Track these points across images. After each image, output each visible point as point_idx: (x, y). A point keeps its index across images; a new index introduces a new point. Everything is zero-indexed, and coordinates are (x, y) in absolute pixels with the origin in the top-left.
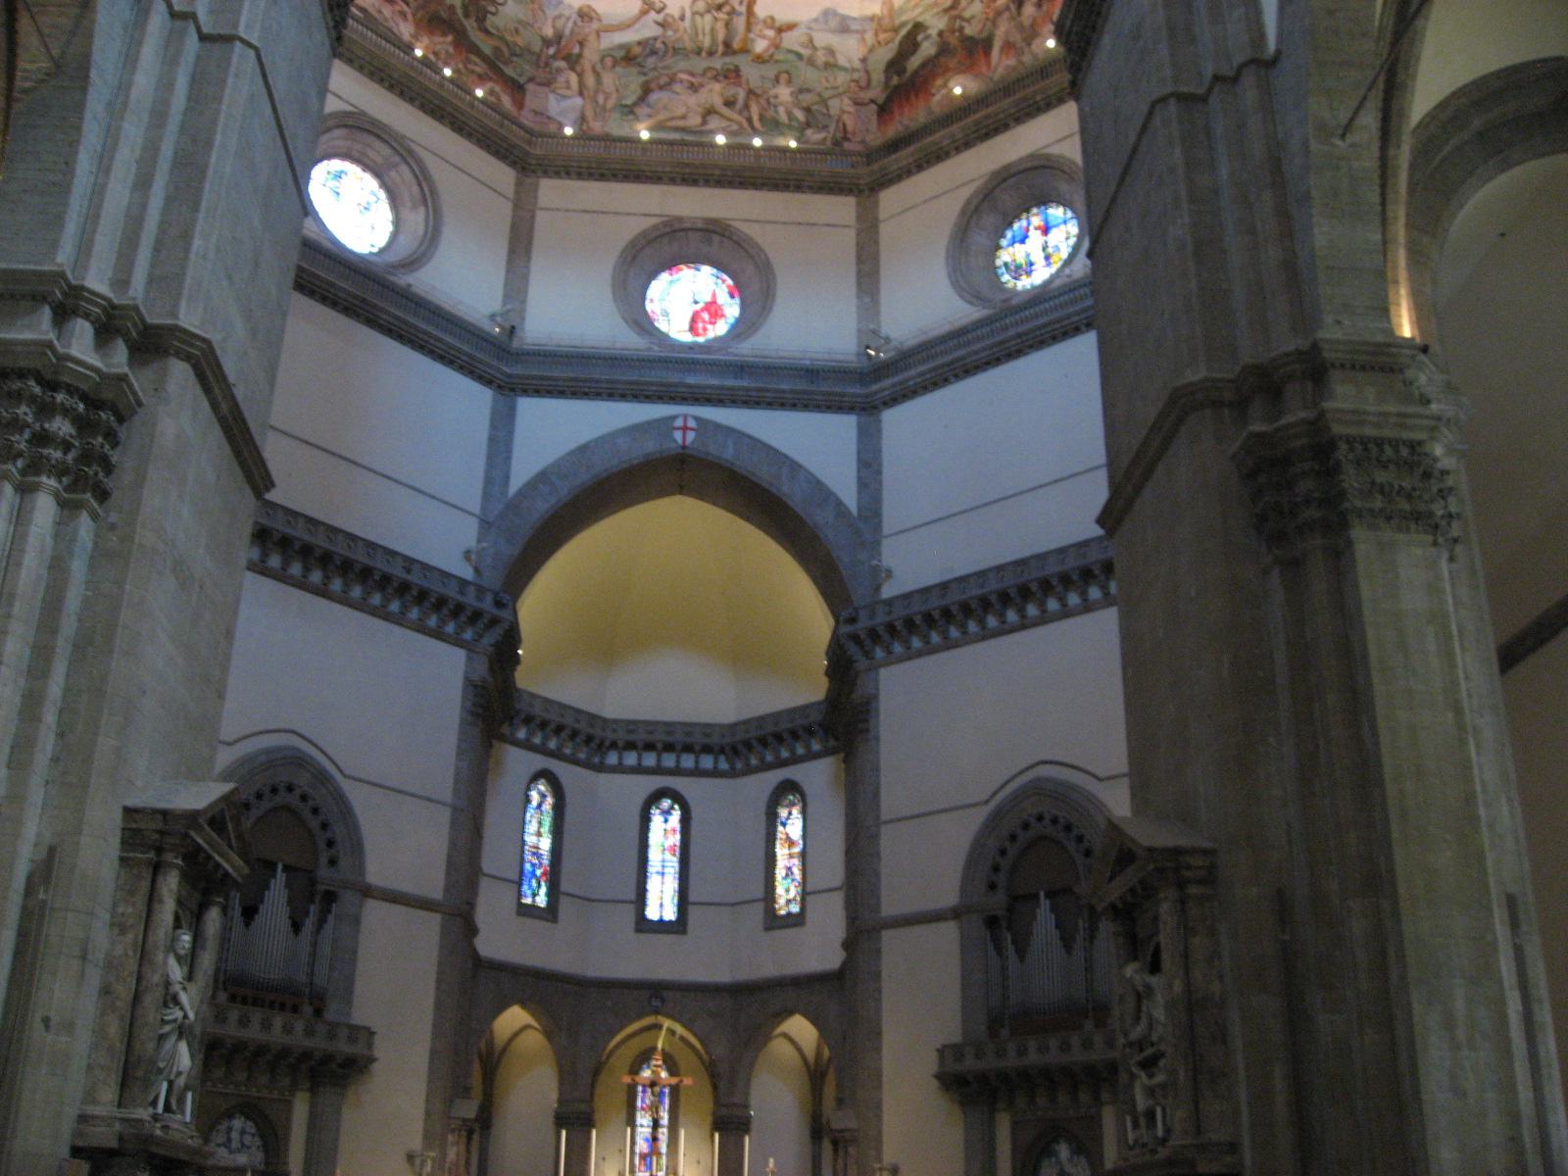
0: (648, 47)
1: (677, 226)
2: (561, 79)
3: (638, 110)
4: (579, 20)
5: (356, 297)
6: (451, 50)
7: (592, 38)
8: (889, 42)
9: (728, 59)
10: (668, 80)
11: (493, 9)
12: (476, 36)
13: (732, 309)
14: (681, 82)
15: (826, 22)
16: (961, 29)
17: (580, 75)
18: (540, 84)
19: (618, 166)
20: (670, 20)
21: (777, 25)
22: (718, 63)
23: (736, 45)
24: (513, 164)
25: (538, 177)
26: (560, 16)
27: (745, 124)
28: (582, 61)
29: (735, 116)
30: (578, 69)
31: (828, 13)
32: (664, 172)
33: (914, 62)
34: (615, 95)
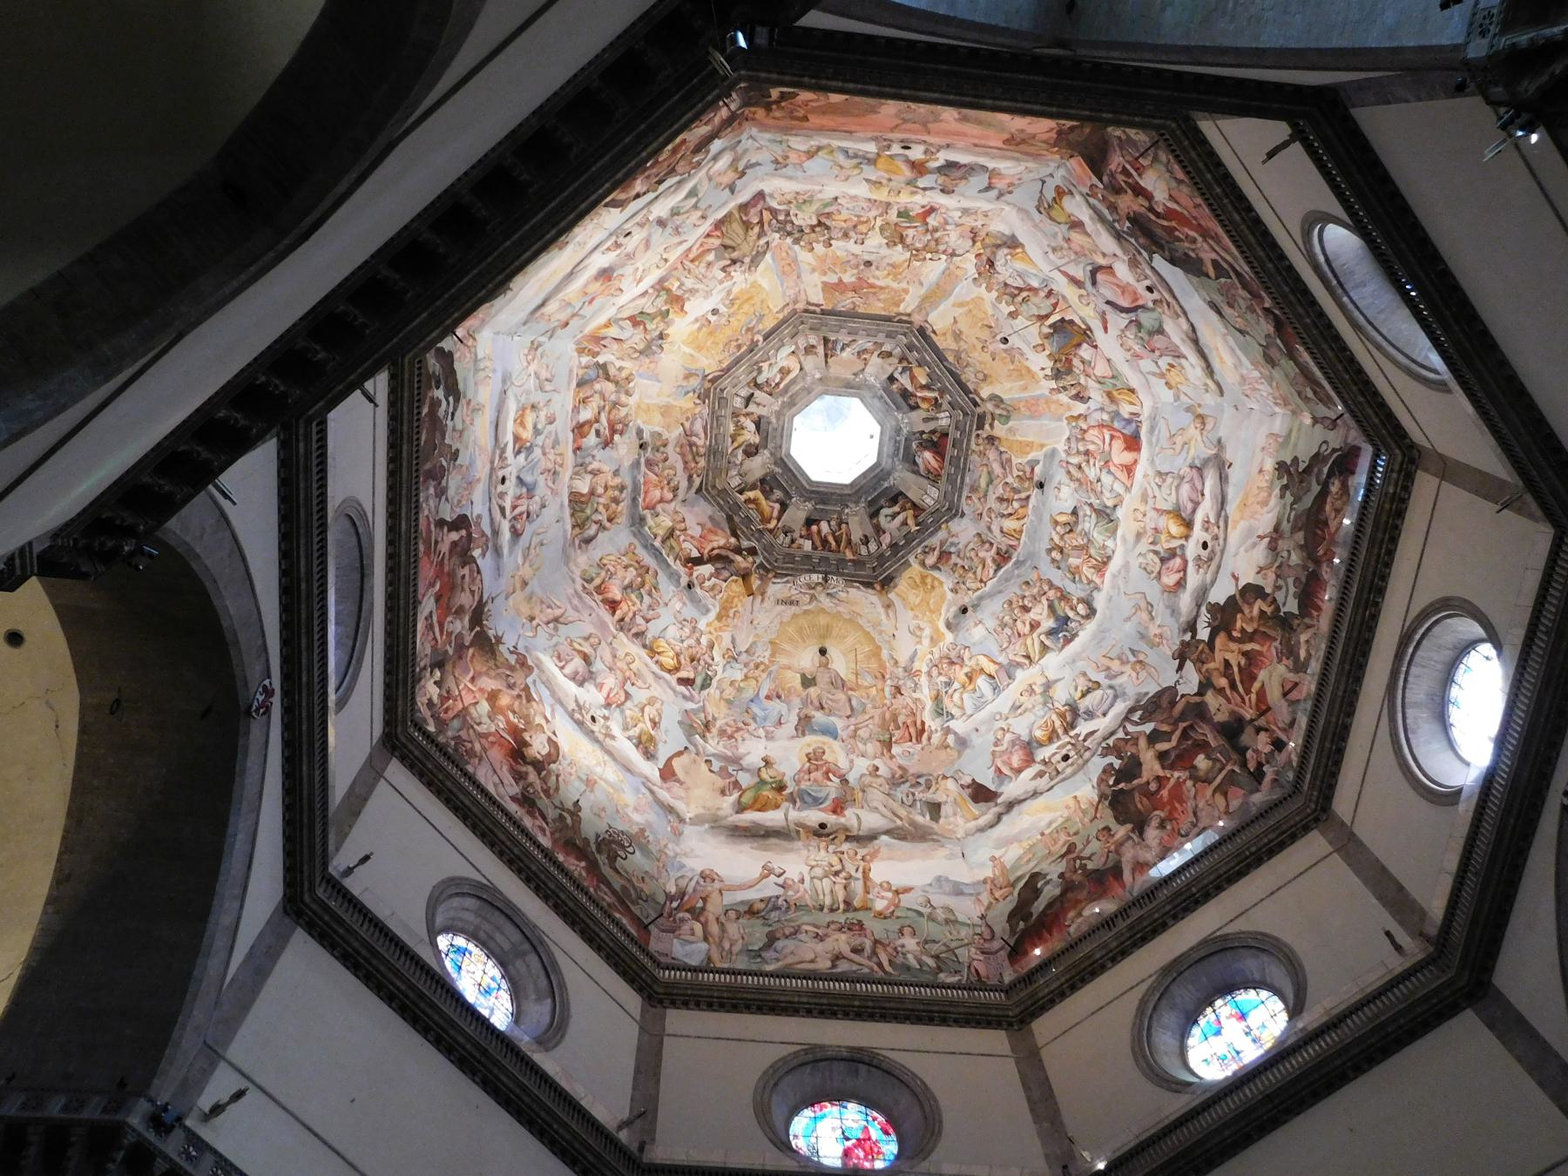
0: (771, 904)
1: (819, 1055)
2: (686, 927)
5: (477, 1046)
6: (584, 874)
7: (715, 895)
9: (850, 915)
11: (621, 853)
12: (606, 870)
13: (890, 1148)
15: (940, 887)
16: (1083, 867)
17: (705, 925)
18: (663, 931)
19: (749, 996)
20: (790, 882)
23: (856, 903)
24: (640, 990)
25: (665, 1008)
26: (682, 877)
27: (876, 968)
28: (706, 913)
30: (702, 919)
31: (939, 879)
32: (799, 1003)
33: (1039, 906)
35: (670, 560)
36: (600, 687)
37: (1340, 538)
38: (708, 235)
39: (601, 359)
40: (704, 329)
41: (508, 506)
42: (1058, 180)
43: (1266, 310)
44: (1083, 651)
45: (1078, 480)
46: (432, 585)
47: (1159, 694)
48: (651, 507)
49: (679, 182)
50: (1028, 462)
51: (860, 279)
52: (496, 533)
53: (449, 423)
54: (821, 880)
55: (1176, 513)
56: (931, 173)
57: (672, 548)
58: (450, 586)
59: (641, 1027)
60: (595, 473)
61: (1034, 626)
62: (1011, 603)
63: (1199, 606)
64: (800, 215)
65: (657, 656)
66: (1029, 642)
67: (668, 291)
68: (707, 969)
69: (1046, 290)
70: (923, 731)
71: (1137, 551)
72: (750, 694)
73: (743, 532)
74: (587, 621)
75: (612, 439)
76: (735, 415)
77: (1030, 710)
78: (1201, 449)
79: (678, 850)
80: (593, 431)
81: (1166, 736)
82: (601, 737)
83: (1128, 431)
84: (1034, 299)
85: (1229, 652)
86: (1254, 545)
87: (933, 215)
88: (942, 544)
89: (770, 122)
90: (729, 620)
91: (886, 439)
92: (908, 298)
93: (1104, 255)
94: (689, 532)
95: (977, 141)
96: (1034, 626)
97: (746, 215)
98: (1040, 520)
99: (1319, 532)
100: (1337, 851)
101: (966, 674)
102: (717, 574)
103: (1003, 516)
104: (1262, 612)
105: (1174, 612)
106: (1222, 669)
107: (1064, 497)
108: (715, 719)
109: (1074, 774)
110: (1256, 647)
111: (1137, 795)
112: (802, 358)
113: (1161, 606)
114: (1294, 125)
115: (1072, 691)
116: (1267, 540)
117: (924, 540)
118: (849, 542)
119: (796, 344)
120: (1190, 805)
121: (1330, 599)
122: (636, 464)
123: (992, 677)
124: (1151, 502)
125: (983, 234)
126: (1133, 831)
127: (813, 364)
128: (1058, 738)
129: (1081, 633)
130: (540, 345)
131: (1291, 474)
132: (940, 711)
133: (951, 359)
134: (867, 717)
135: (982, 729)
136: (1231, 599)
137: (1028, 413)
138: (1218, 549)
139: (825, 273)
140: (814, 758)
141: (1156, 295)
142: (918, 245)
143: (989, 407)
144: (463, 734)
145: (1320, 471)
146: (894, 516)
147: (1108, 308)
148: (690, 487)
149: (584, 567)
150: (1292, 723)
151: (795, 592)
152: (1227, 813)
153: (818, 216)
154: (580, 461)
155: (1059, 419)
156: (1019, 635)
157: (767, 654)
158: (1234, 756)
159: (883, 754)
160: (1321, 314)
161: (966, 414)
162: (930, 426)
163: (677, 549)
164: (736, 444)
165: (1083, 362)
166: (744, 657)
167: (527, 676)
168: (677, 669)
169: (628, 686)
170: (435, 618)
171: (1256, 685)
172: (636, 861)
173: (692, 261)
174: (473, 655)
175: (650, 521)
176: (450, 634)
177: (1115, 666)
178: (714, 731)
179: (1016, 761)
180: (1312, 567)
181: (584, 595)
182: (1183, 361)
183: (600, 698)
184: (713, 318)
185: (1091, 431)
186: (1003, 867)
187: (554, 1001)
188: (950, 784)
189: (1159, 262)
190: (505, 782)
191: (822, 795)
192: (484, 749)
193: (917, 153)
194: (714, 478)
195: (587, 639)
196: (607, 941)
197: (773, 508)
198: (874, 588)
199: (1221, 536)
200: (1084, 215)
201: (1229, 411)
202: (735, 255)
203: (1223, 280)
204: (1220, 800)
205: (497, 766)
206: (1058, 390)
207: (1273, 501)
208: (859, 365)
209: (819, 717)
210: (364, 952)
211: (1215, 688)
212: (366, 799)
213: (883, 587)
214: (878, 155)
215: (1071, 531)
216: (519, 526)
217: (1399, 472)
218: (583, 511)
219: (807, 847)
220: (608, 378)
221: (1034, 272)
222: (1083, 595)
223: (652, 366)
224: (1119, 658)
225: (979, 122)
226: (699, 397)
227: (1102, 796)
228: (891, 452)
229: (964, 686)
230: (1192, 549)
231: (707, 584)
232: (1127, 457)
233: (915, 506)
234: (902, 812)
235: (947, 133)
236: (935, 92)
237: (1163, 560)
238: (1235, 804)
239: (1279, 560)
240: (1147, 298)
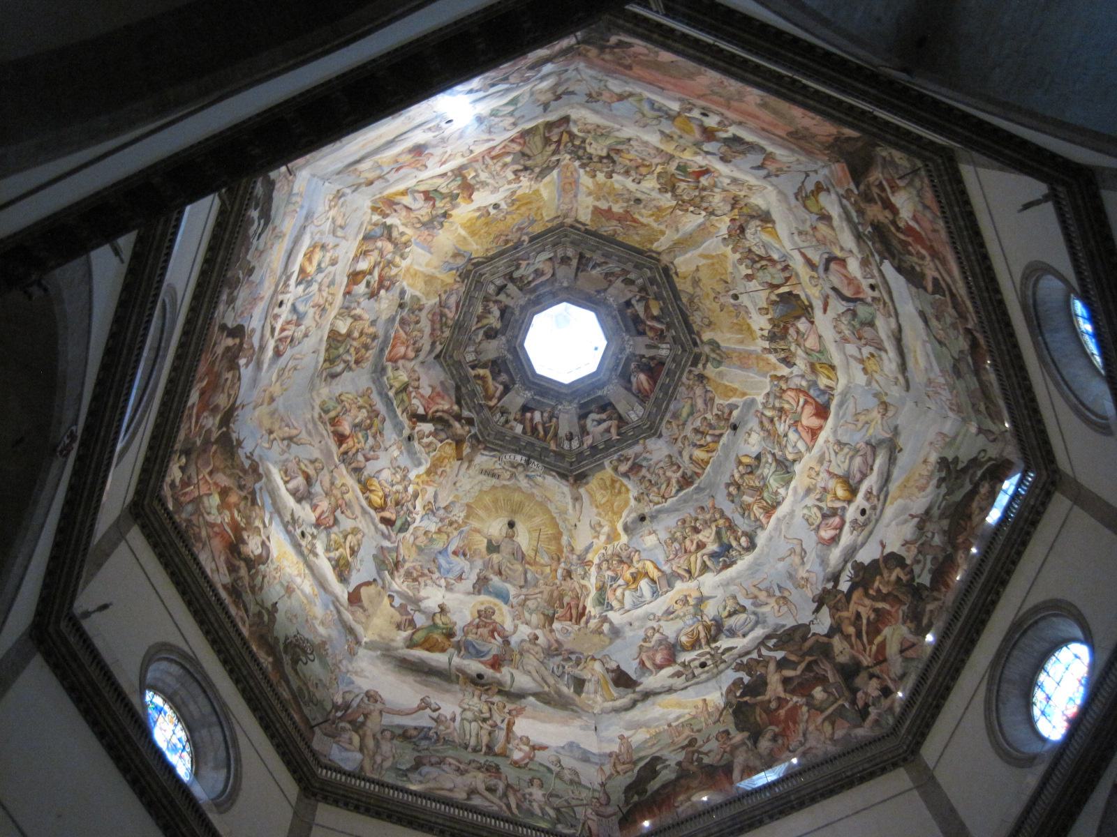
0: (423, 733)
2: (346, 736)
3: (410, 775)
4: (366, 700)
7: (376, 714)
8: (625, 773)
9: (490, 758)
10: (437, 759)
11: (304, 659)
12: (288, 669)
14: (450, 764)
15: (571, 751)
17: (362, 739)
18: (325, 734)
19: (394, 808)
20: (443, 719)
21: (531, 744)
22: (482, 760)
23: (497, 749)
24: (299, 781)
25: (318, 801)
26: (349, 692)
27: (504, 807)
28: (365, 728)
29: (496, 800)
30: (361, 732)
31: (571, 745)
32: (435, 823)
33: (655, 785)
34: (391, 759)
35: (399, 412)
36: (314, 508)
37: (979, 532)
38: (513, 141)
39: (389, 221)
40: (483, 219)
41: (278, 327)
43: (968, 331)
44: (738, 578)
45: (768, 431)
46: (201, 380)
47: (795, 629)
48: (394, 360)
50: (729, 405)
51: (627, 212)
52: (262, 348)
53: (255, 242)
54: (470, 722)
55: (845, 480)
57: (402, 401)
58: (215, 385)
59: (295, 813)
60: (357, 318)
61: (700, 546)
62: (684, 522)
63: (846, 562)
64: (594, 145)
65: (368, 494)
66: (693, 559)
67: (464, 178)
68: (358, 775)
69: (784, 264)
70: (583, 614)
71: (803, 504)
72: (439, 546)
73: (466, 404)
74: (318, 446)
75: (378, 292)
76: (486, 299)
77: (681, 618)
78: (878, 430)
79: (350, 668)
80: (364, 282)
81: (793, 665)
82: (306, 552)
83: (821, 400)
84: (771, 270)
85: (863, 607)
86: (906, 521)
87: (706, 176)
88: (637, 456)
89: (601, 62)
90: (437, 477)
91: (610, 353)
92: (662, 239)
93: (842, 249)
94: (421, 391)
95: (765, 126)
96: (700, 546)
97: (550, 131)
98: (727, 456)
99: (962, 522)
100: (917, 788)
101: (632, 574)
102: (435, 434)
103: (695, 445)
104: (899, 579)
105: (824, 562)
106: (853, 619)
107: (753, 443)
108: (404, 561)
109: (708, 680)
110: (887, 607)
111: (758, 710)
112: (557, 266)
113: (814, 554)
114: (1052, 189)
115: (721, 610)
116: (916, 520)
117: (623, 449)
118: (556, 435)
119: (555, 252)
120: (802, 727)
121: (961, 581)
122: (391, 320)
123: (653, 581)
124: (826, 464)
125: (742, 203)
126: (749, 738)
127: (565, 273)
128: (700, 647)
129: (740, 563)
130: (343, 195)
131: (949, 470)
132: (601, 601)
133: (685, 300)
134: (537, 591)
135: (636, 624)
136: (875, 563)
137: (738, 363)
138: (874, 518)
139: (598, 199)
140: (485, 616)
141: (876, 294)
142: (685, 197)
143: (707, 349)
144: (194, 519)
145: (975, 472)
146: (600, 422)
147: (831, 293)
148: (431, 351)
149: (324, 397)
150: (903, 677)
151: (497, 466)
152: (832, 739)
153: (610, 149)
154: (346, 304)
155: (764, 375)
156: (686, 551)
157: (462, 515)
158: (847, 694)
159: (544, 626)
160: (1015, 346)
161: (684, 350)
162: (652, 353)
163: (407, 403)
164: (480, 325)
165: (798, 332)
166: (441, 512)
167: (256, 482)
168: (382, 508)
169: (339, 511)
170: (195, 411)
171: (879, 639)
172: (314, 668)
173: (493, 158)
174: (215, 452)
175: (390, 372)
176: (202, 427)
177: (762, 596)
178: (402, 571)
179: (659, 658)
180: (950, 550)
181: (319, 423)
182: (883, 354)
183: (313, 517)
184: (493, 212)
185: (789, 393)
186: (629, 746)
187: (229, 772)
188: (597, 666)
189: (887, 267)
190: (221, 570)
191: (485, 649)
192: (209, 536)
193: (712, 121)
194: (453, 350)
195: (312, 462)
196: (281, 731)
197: (497, 388)
198: (568, 481)
199: (879, 507)
200: (835, 211)
201: (910, 404)
202: (529, 163)
203: (937, 296)
204: (828, 728)
205: (216, 554)
206: (769, 351)
207: (930, 489)
208: (604, 284)
209: (495, 580)
210: (89, 689)
211: (842, 632)
212: (108, 555)
213: (575, 481)
214: (679, 114)
215: (751, 473)
216: (281, 348)
217: (1042, 489)
218: (337, 348)
219: (463, 691)
220: (390, 239)
221: (777, 246)
222: (747, 529)
223: (429, 238)
224: (767, 590)
225: (775, 112)
226: (460, 276)
227: (728, 704)
228: (611, 366)
229: (627, 584)
230: (851, 513)
231: (425, 440)
232: (815, 422)
233: (620, 418)
234: (551, 681)
235: (743, 113)
236: (758, 76)
237: (824, 516)
238: (839, 734)
239: (924, 538)
240: (869, 294)
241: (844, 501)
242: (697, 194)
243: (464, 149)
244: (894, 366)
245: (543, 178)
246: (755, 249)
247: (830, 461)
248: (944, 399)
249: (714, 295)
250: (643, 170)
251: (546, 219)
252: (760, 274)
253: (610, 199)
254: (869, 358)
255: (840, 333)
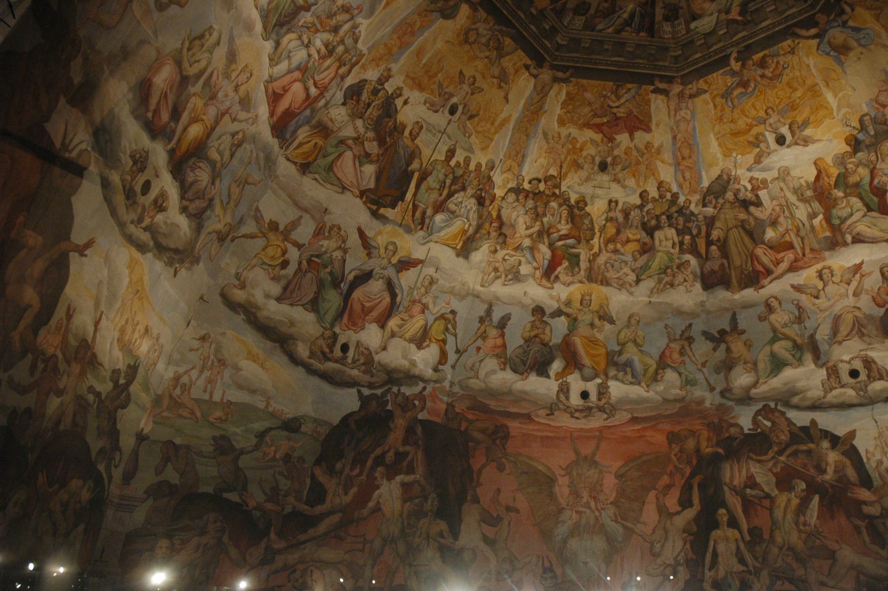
38: (769, 272)
40: (800, 119)
42: (447, 368)
45: (335, 14)
49: (788, 404)
55: (198, 150)
56: (558, 346)
67: (828, 219)
69: (427, 221)
84: (434, 196)
86: (97, 305)
92: (558, 111)
93: (393, 335)
119: (688, 30)
125: (494, 234)
133: (508, 41)
138: (128, 217)
139: (648, 145)
142: (554, 204)
173: (790, 246)
184: (785, 130)
185: (332, 75)
202: (743, 216)
206: (382, 81)
241: (179, 140)
242: (545, 220)
243: (831, 289)
244: (259, 297)
245: (720, 177)
246: (459, 197)
247: (234, 120)
248: (194, 374)
249: (476, 85)
250: (611, 230)
251: (707, 96)
252: (441, 177)
253: (635, 153)
254: (284, 252)
255: (331, 229)
